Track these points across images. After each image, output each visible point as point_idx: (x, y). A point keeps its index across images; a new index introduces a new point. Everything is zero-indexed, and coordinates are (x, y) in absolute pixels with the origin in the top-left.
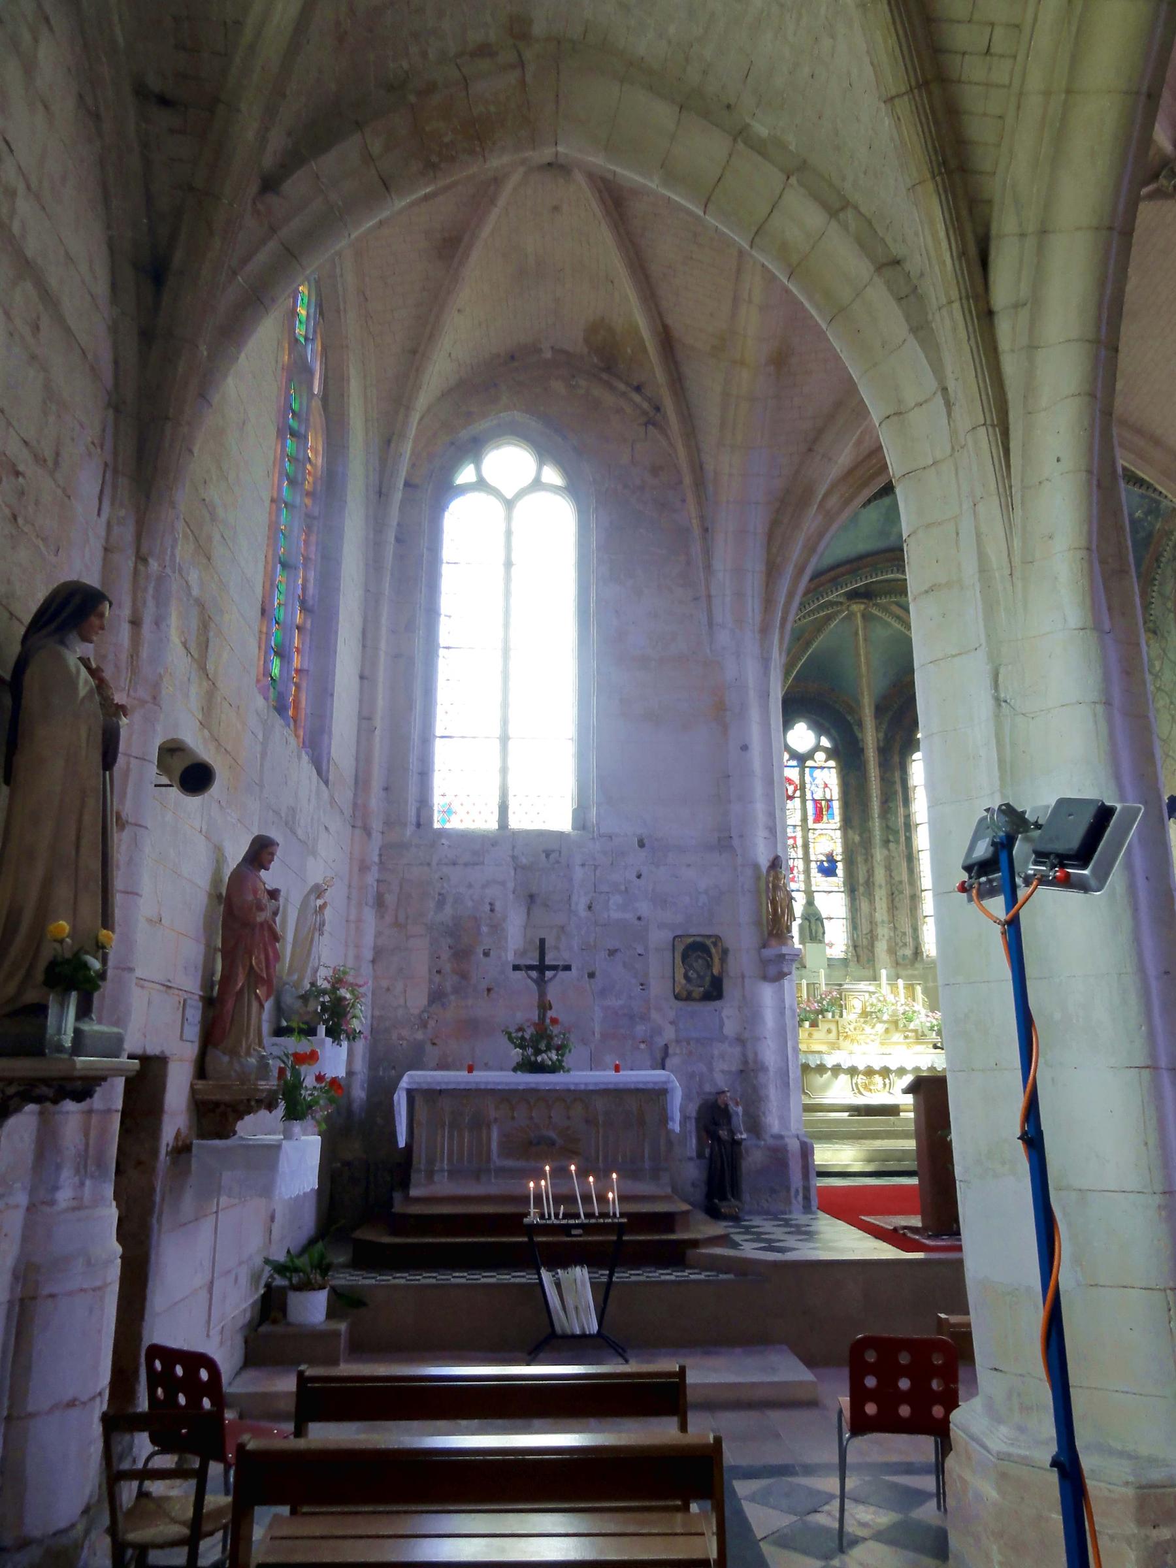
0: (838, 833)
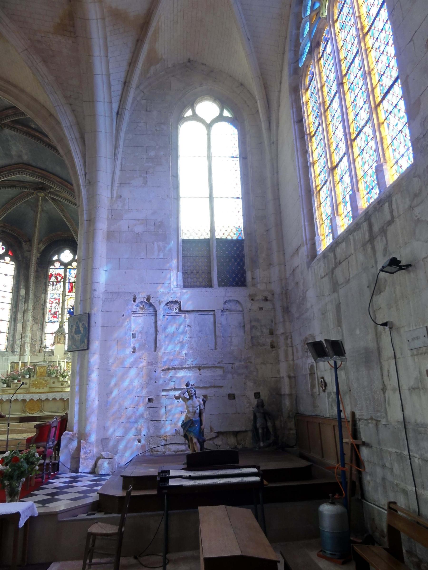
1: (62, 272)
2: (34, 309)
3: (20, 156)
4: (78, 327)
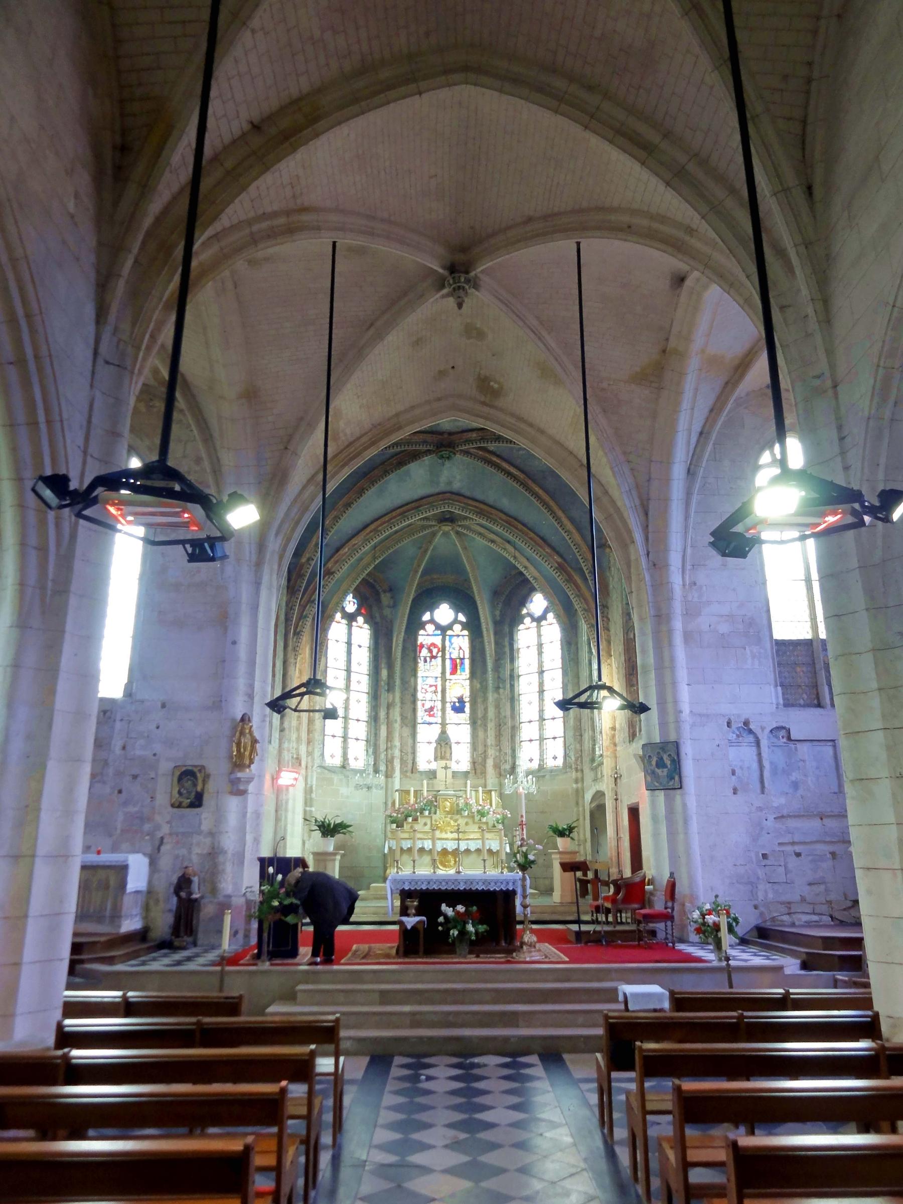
0: (468, 682)
1: (438, 640)
2: (402, 702)
3: (450, 483)
4: (661, 759)
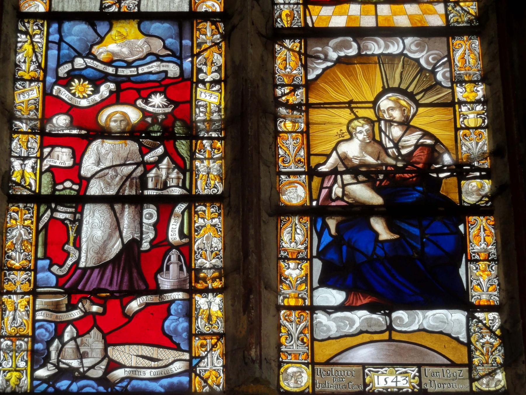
0: (468, 53)
